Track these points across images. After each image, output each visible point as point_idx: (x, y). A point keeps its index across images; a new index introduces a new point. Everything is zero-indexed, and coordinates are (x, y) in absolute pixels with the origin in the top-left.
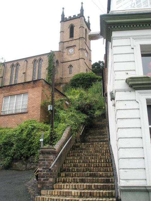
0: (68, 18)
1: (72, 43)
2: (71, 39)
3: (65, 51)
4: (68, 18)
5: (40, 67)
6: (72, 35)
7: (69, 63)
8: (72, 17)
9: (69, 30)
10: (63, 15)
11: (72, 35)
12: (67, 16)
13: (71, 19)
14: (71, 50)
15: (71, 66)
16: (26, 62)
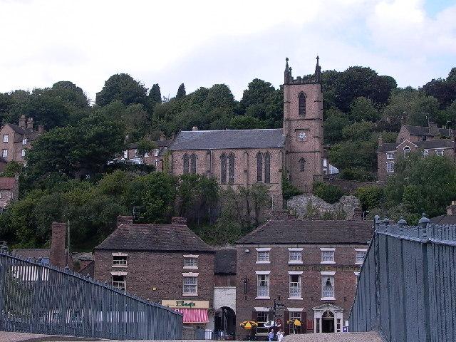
0: (295, 78)
1: (305, 125)
2: (302, 117)
3: (294, 134)
4: (295, 78)
5: (268, 166)
6: (302, 111)
7: (300, 155)
8: (302, 77)
9: (297, 100)
10: (288, 73)
11: (302, 111)
12: (295, 75)
13: (300, 81)
14: (303, 135)
15: (303, 160)
16: (246, 154)
